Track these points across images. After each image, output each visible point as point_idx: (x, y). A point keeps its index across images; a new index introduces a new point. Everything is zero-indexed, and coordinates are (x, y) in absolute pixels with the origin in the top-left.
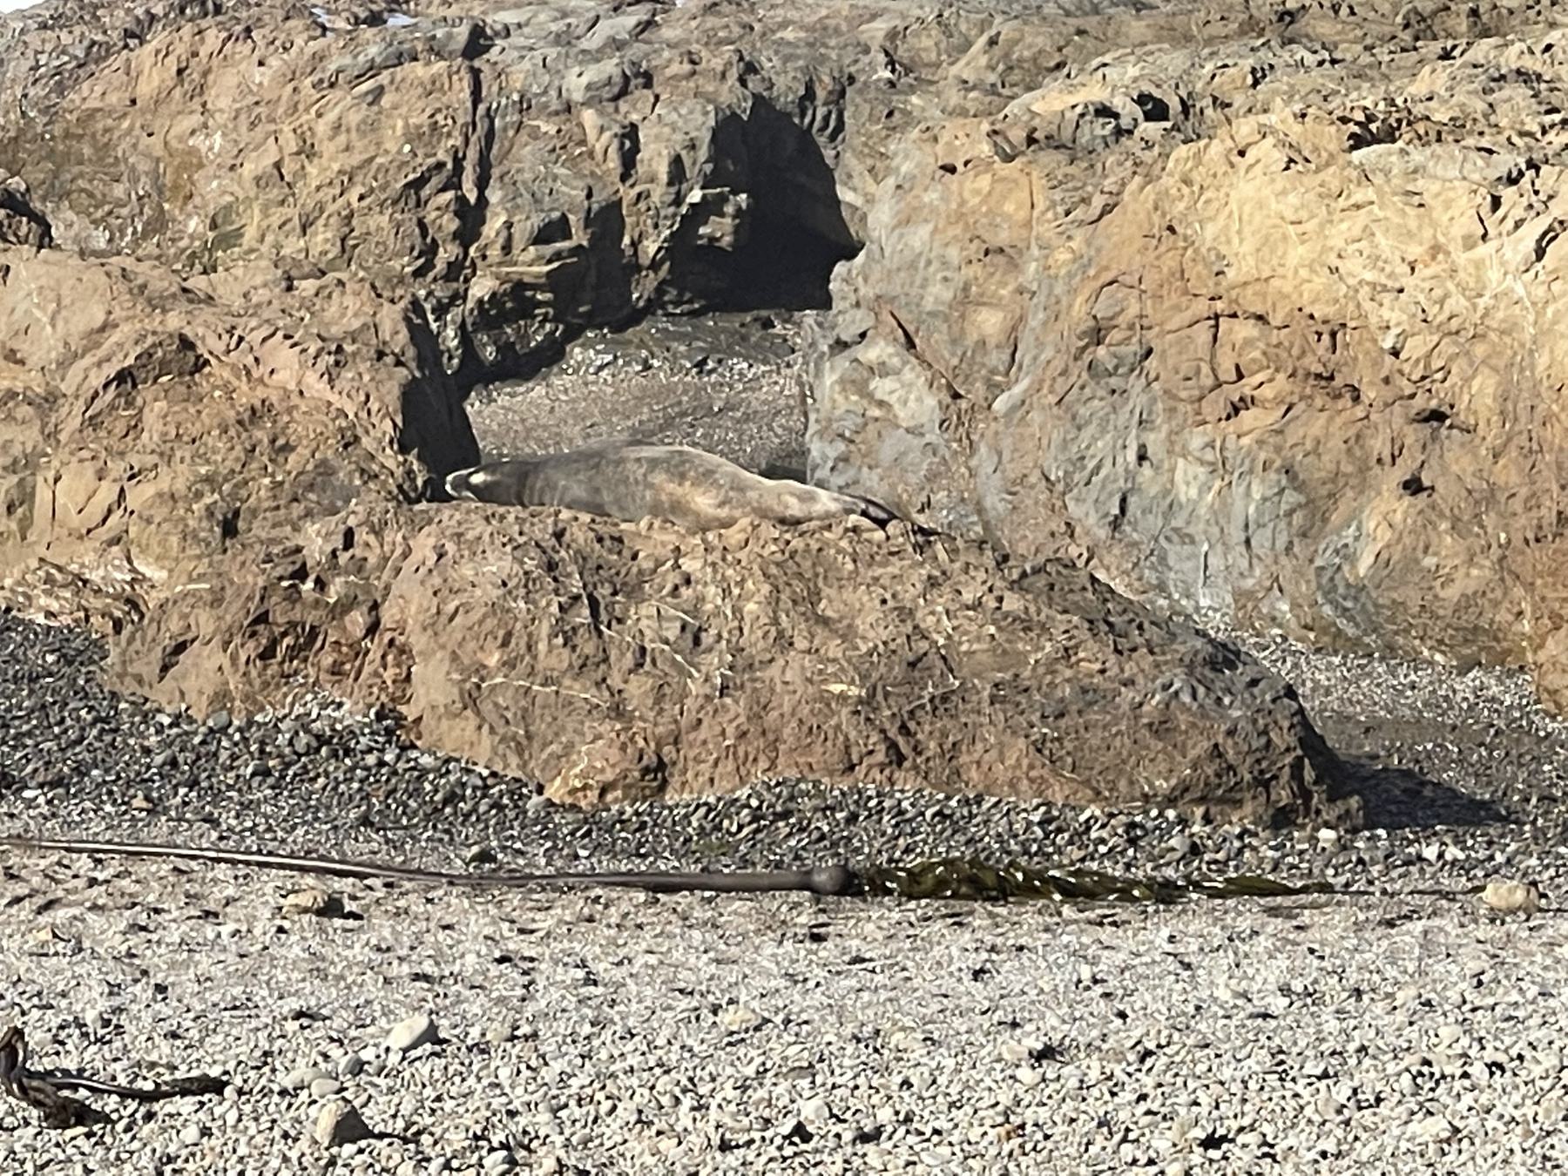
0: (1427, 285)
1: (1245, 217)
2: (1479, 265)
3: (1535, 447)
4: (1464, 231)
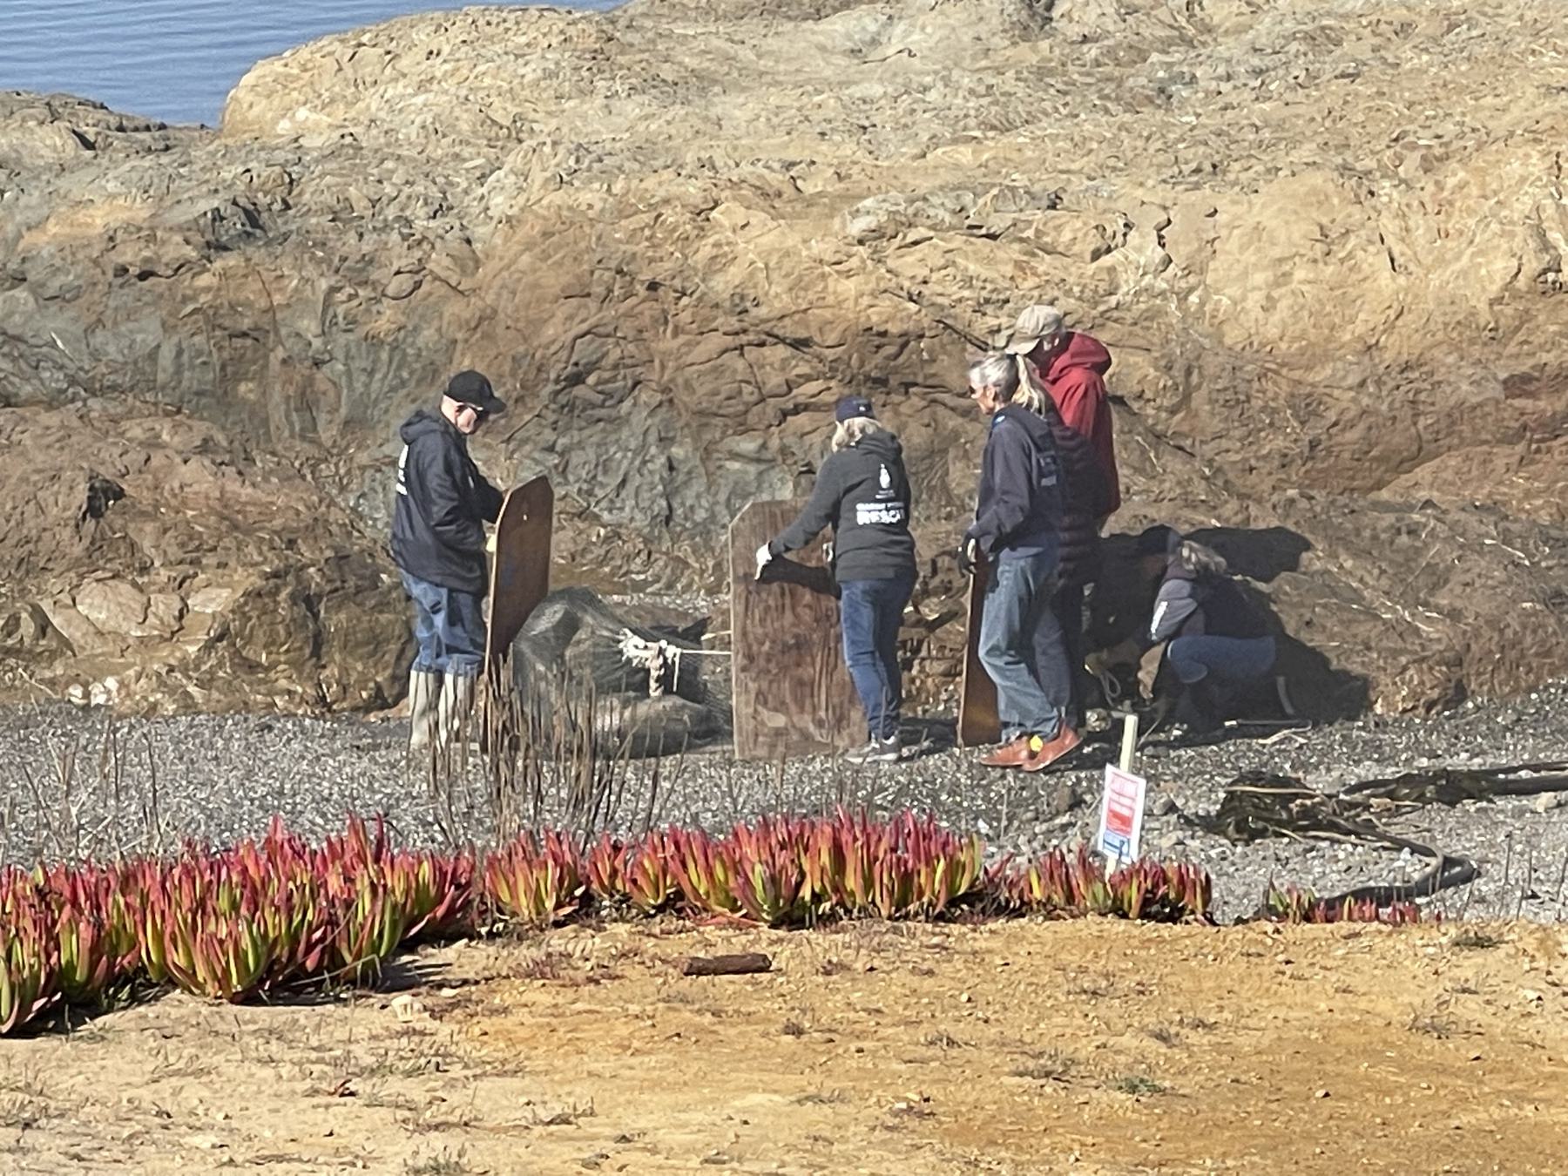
0: (1036, 293)
1: (772, 265)
2: (1111, 270)
3: (1242, 398)
4: (1092, 247)
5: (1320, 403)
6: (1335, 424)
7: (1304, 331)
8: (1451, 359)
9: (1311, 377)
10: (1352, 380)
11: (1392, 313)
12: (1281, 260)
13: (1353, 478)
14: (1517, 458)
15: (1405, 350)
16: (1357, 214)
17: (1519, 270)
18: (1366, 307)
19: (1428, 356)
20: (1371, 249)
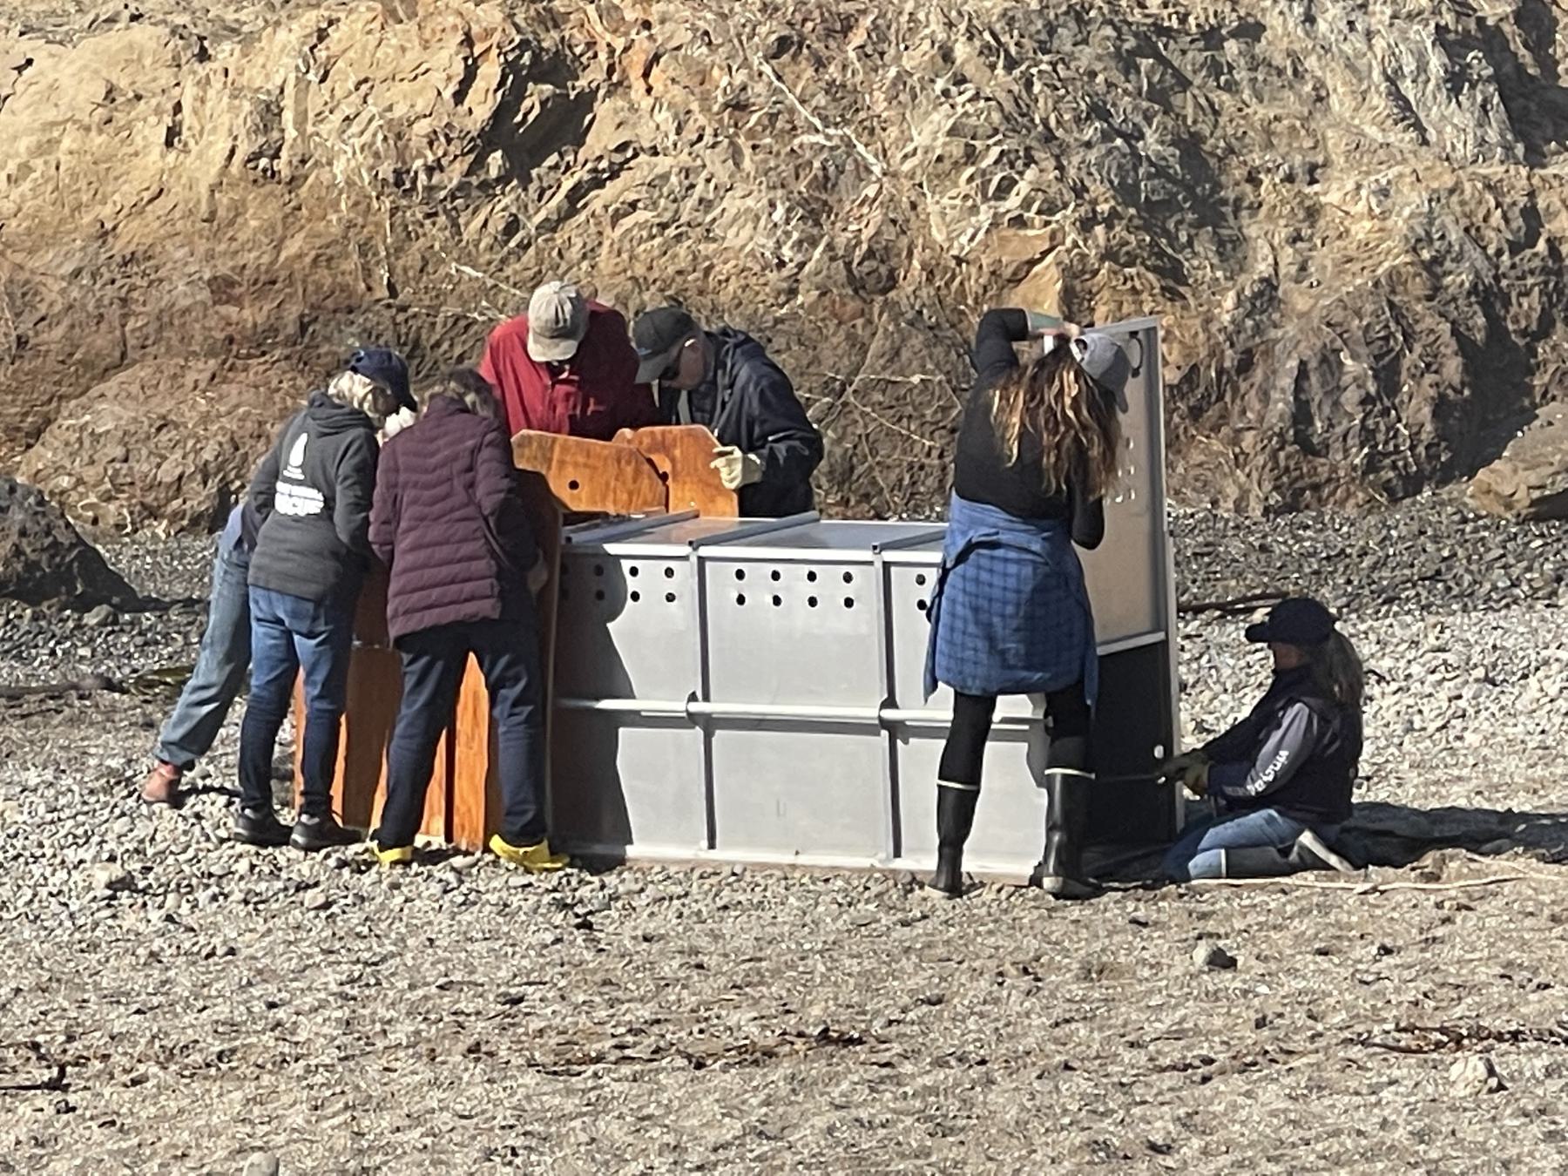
5: (35, 294)
6: (43, 319)
7: (39, 209)
8: (180, 254)
9: (35, 263)
10: (68, 268)
11: (147, 196)
12: (54, 124)
13: (58, 383)
14: (208, 375)
15: (136, 240)
16: (166, 77)
17: (232, 152)
18: (126, 188)
19: (159, 249)
20: (153, 120)
